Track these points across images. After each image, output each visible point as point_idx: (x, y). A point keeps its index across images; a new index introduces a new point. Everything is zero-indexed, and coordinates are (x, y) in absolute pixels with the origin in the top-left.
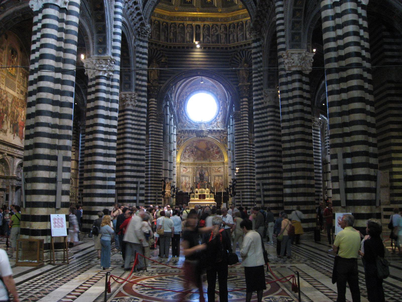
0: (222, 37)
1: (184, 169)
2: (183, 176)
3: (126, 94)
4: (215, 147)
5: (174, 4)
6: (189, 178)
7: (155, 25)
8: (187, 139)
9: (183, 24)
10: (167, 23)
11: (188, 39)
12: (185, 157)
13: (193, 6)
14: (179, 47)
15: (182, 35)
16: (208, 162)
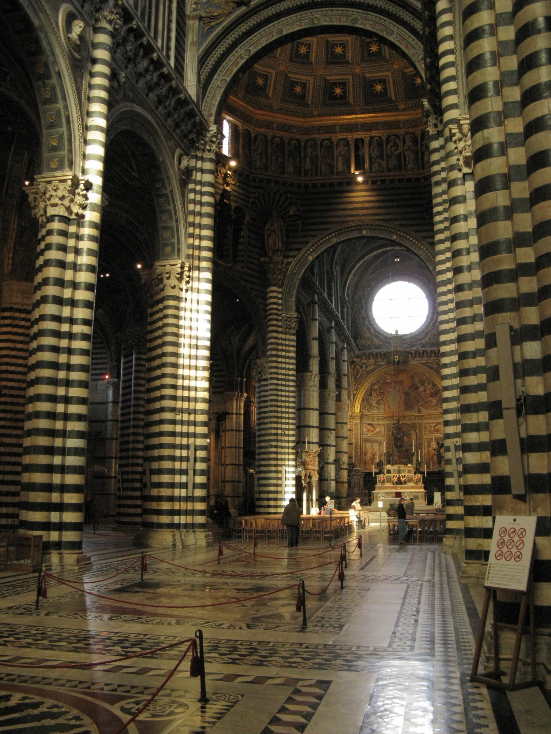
0: (407, 159)
1: (370, 427)
2: (367, 441)
3: (165, 266)
4: (429, 384)
5: (310, 102)
6: (380, 444)
7: (274, 145)
8: (372, 370)
9: (329, 140)
10: (298, 140)
11: (340, 167)
12: (371, 405)
13: (348, 104)
14: (323, 185)
15: (329, 161)
16: (416, 414)
